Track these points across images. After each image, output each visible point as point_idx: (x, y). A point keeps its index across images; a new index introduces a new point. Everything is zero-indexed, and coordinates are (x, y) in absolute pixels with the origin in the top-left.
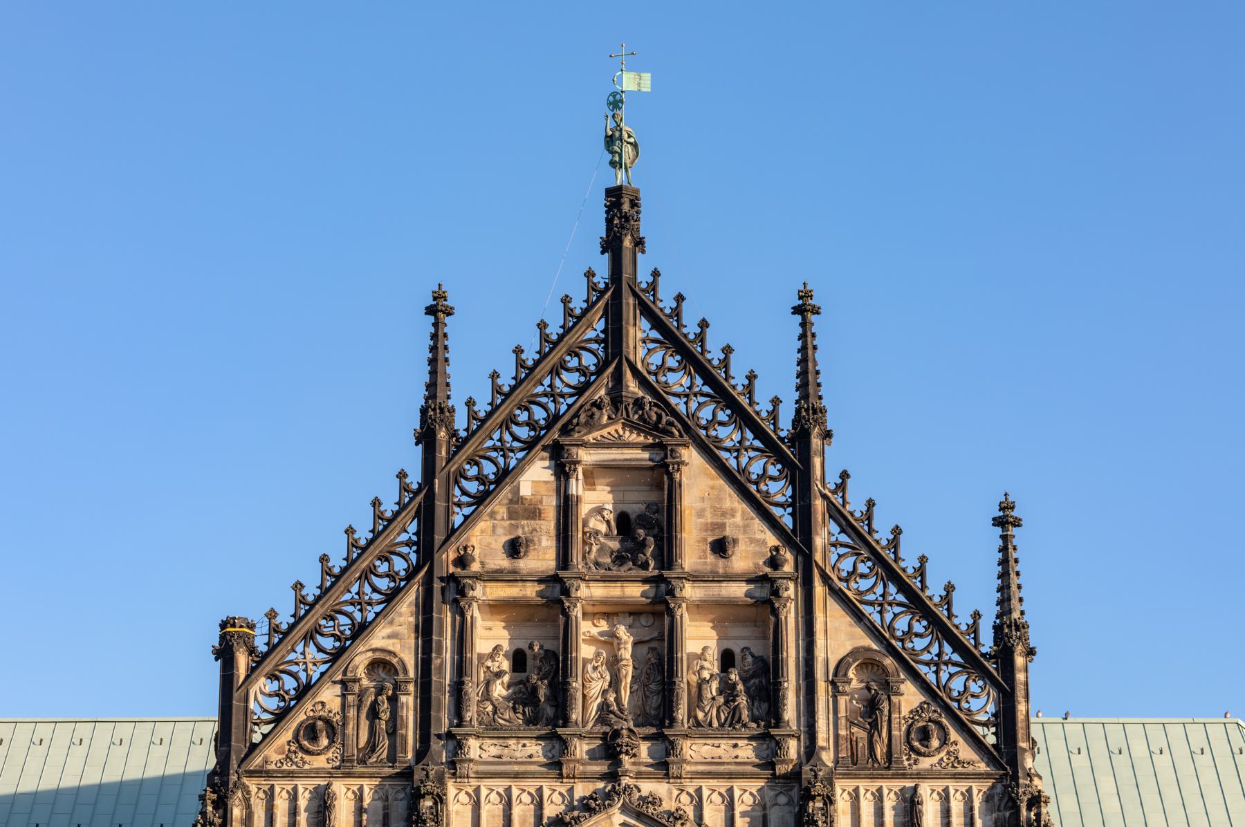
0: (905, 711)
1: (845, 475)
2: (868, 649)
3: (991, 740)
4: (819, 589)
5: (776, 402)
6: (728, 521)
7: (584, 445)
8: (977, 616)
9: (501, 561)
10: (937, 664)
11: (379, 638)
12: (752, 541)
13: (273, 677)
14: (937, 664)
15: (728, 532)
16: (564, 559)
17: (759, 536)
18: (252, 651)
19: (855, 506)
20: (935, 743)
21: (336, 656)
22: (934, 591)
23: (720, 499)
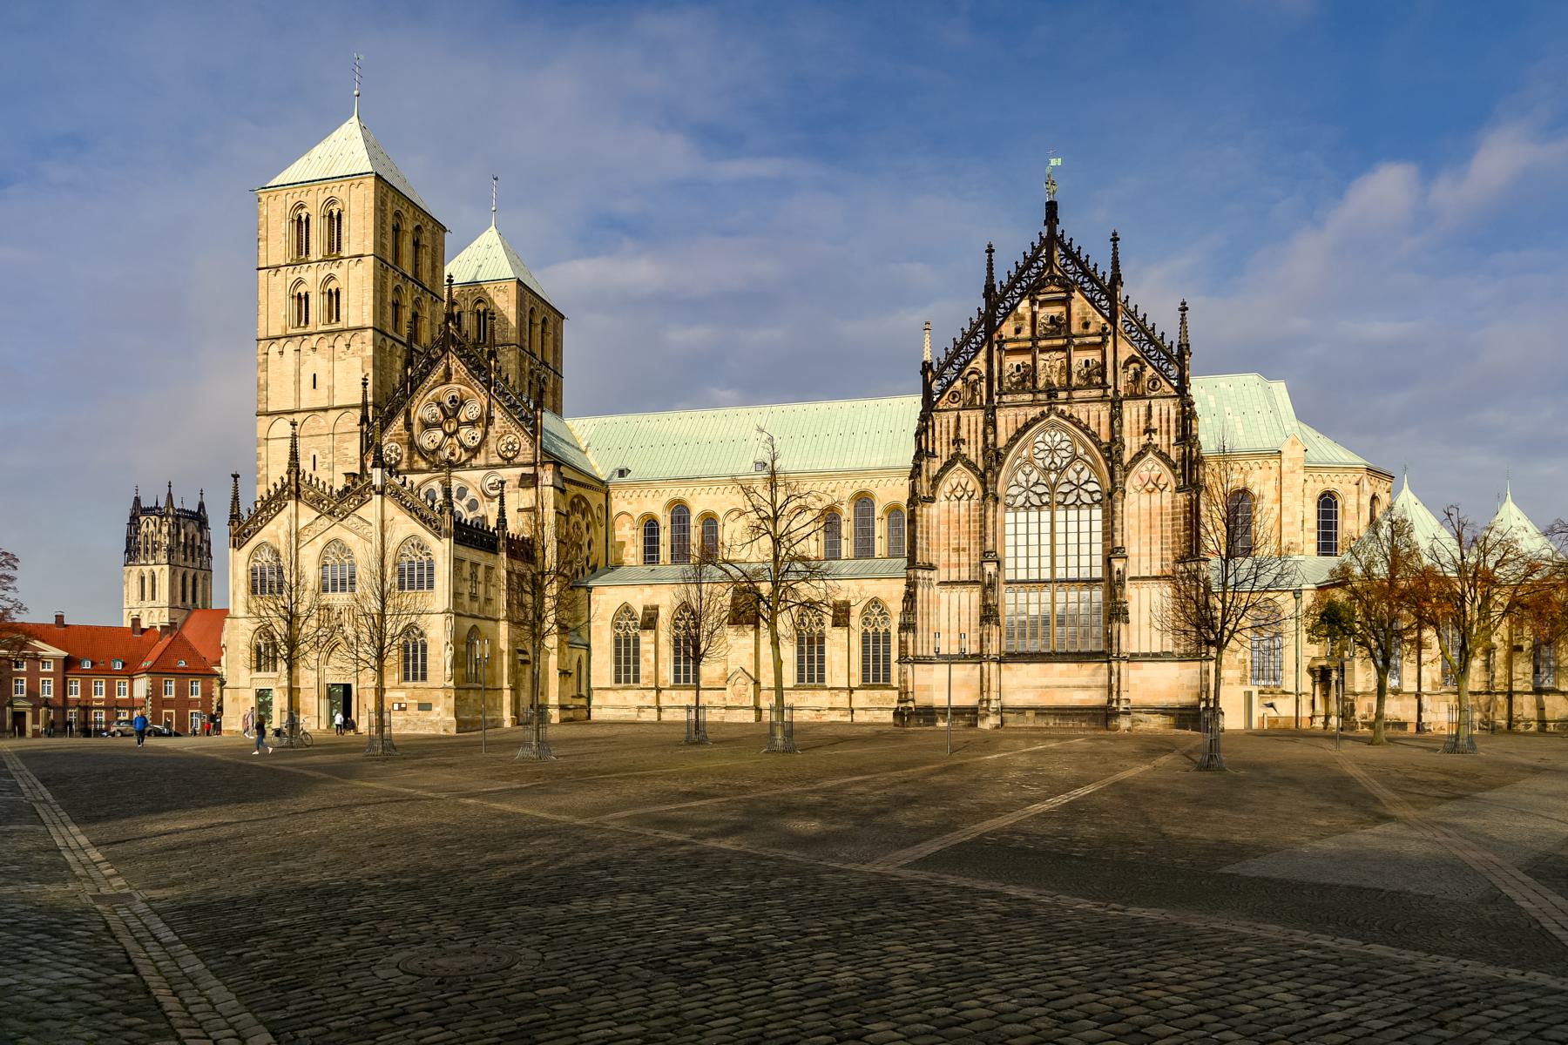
1: (1127, 297)
3: (1176, 384)
4: (1118, 337)
5: (1104, 273)
7: (1039, 294)
8: (1172, 343)
9: (1011, 335)
11: (972, 365)
13: (939, 379)
14: (1159, 359)
16: (1033, 332)
18: (933, 372)
19: (1132, 308)
20: (1157, 387)
21: (960, 371)
22: (1158, 335)
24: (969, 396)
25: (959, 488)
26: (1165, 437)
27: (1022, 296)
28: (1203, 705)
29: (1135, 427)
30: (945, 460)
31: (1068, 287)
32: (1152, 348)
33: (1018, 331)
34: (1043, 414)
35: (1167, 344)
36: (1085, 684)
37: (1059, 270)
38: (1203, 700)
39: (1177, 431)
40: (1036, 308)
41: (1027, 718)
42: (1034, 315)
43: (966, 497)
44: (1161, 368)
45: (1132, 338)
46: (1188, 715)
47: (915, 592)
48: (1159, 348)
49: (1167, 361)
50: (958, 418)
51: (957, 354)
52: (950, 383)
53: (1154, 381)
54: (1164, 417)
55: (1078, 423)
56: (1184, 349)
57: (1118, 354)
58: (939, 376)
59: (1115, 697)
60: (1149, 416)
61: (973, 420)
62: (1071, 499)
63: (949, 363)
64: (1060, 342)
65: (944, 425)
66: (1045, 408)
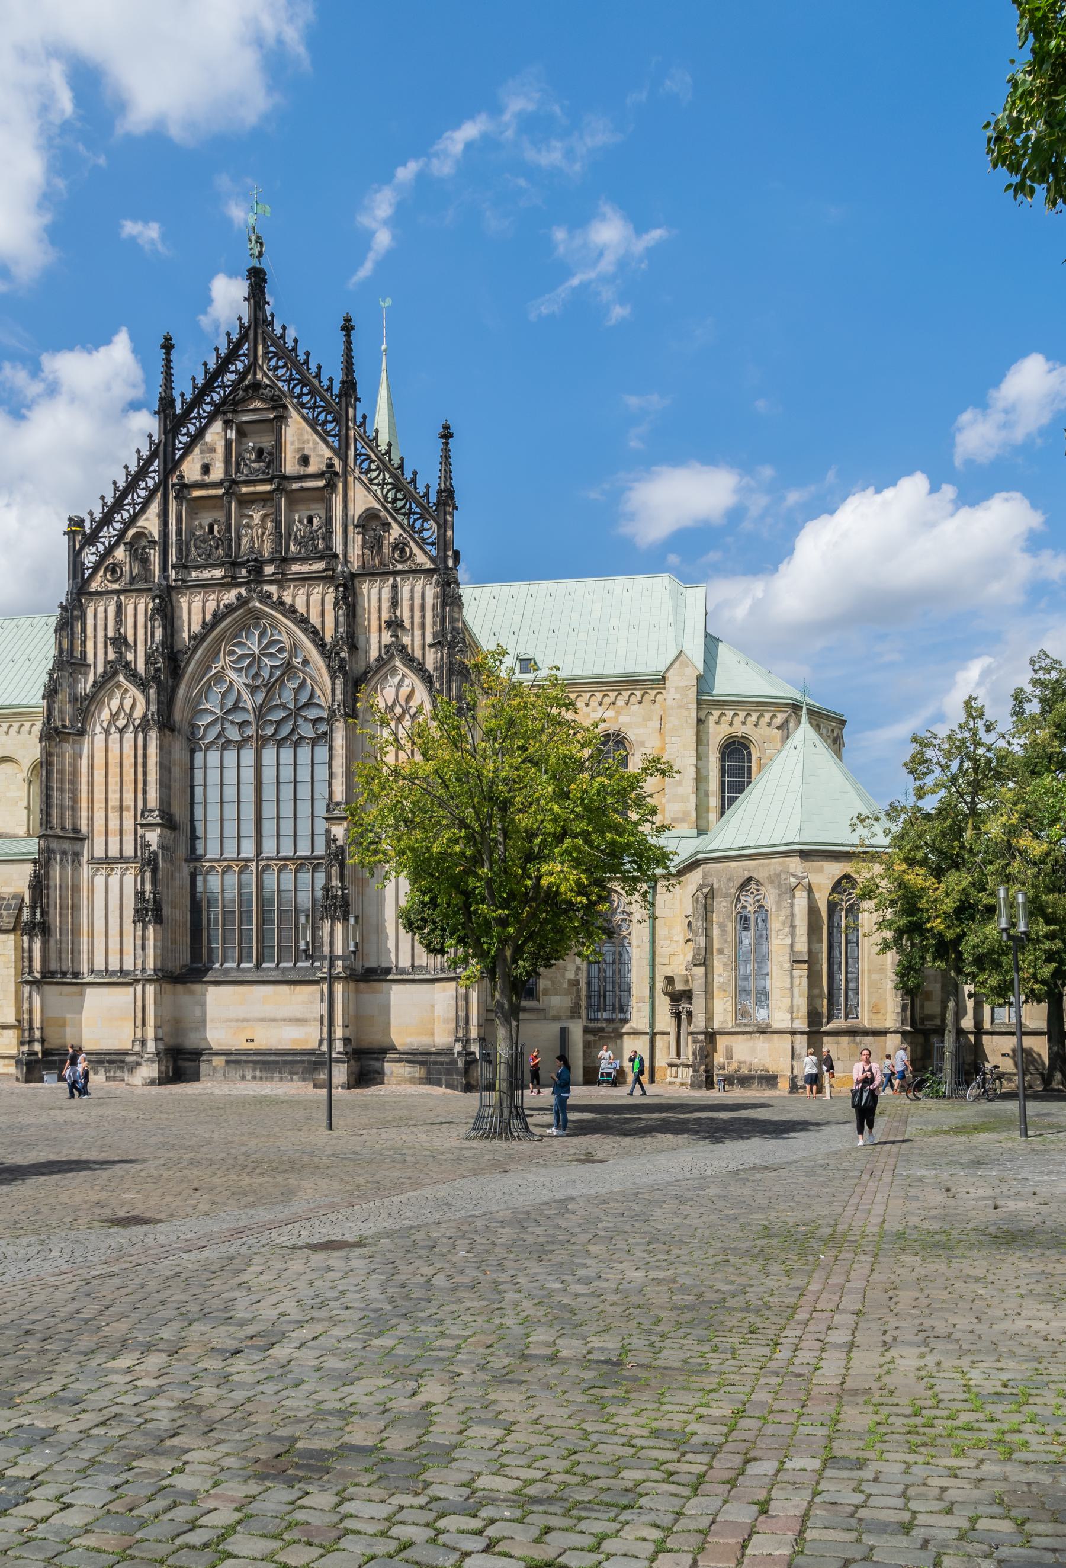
0: (392, 540)
2: (373, 508)
4: (351, 479)
5: (331, 380)
6: (306, 446)
7: (235, 412)
8: (428, 487)
10: (408, 514)
11: (139, 524)
12: (318, 456)
14: (408, 514)
15: (306, 452)
16: (227, 471)
17: (321, 453)
22: (408, 476)
23: (302, 435)
24: (135, 571)
25: (122, 715)
26: (417, 633)
27: (211, 418)
28: (458, 1047)
29: (374, 617)
30: (100, 669)
31: (277, 404)
32: (399, 496)
33: (206, 469)
34: (239, 597)
35: (422, 490)
36: (298, 1015)
37: (265, 374)
38: (457, 1040)
39: (434, 623)
40: (232, 434)
41: (215, 1068)
42: (228, 444)
43: (131, 728)
44: (413, 527)
45: (371, 480)
46: (442, 1063)
47: (47, 873)
48: (409, 497)
49: (422, 516)
50: (119, 607)
51: (118, 504)
52: (110, 550)
53: (400, 547)
54: (417, 602)
55: (291, 611)
56: (447, 495)
57: (351, 505)
58: (91, 539)
59: (325, 1035)
60: (395, 603)
61: (141, 607)
62: (285, 731)
63: (107, 520)
64: (268, 488)
65: (101, 615)
66: (243, 591)
